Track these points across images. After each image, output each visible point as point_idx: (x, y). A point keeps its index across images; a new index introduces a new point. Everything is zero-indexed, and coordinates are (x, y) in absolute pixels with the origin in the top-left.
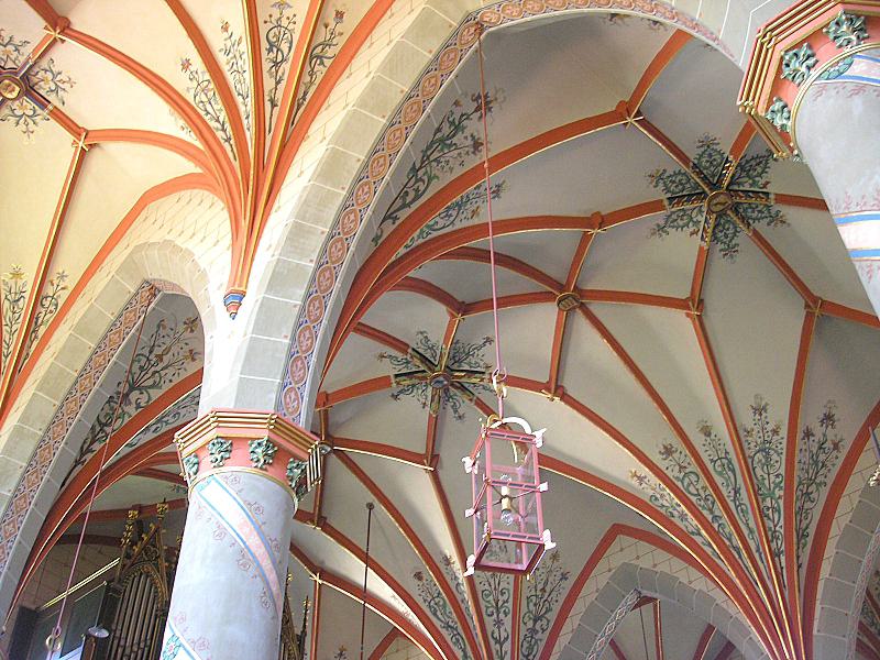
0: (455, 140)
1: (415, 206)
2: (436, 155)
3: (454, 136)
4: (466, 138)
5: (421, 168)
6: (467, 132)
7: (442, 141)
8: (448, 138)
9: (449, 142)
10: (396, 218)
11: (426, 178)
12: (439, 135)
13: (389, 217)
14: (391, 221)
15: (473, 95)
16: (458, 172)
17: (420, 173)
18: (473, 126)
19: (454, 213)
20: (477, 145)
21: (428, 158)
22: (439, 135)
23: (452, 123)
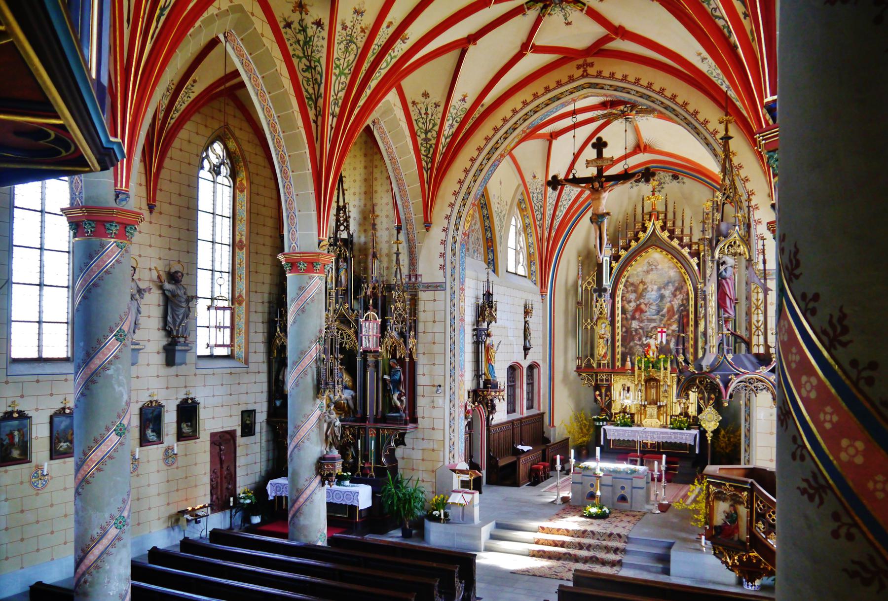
0: (309, 35)
1: (323, 81)
2: (309, 51)
3: (307, 35)
4: (312, 28)
5: (310, 63)
6: (309, 25)
7: (306, 43)
8: (306, 38)
9: (308, 39)
10: (321, 94)
11: (317, 64)
12: (301, 43)
13: (318, 97)
14: (320, 98)
15: (293, 11)
16: (325, 43)
17: (313, 66)
18: (309, 20)
19: (353, 46)
20: (319, 23)
21: (308, 56)
22: (301, 43)
23: (300, 31)
